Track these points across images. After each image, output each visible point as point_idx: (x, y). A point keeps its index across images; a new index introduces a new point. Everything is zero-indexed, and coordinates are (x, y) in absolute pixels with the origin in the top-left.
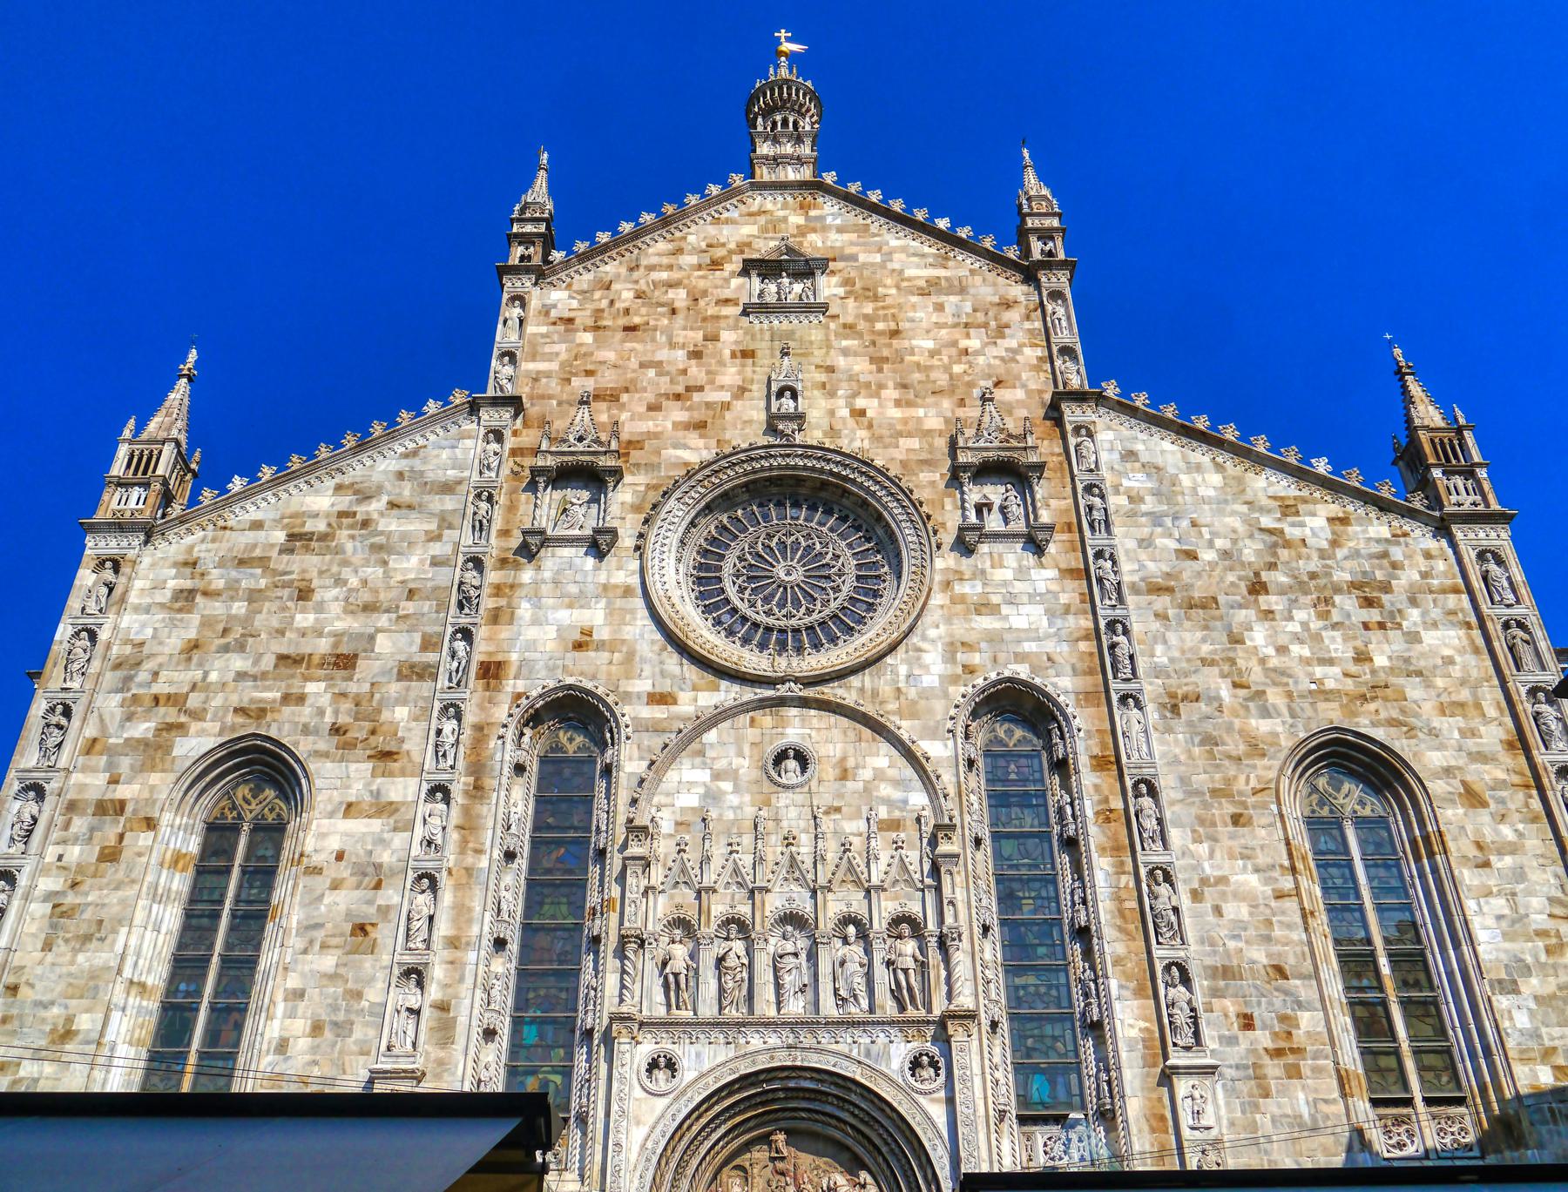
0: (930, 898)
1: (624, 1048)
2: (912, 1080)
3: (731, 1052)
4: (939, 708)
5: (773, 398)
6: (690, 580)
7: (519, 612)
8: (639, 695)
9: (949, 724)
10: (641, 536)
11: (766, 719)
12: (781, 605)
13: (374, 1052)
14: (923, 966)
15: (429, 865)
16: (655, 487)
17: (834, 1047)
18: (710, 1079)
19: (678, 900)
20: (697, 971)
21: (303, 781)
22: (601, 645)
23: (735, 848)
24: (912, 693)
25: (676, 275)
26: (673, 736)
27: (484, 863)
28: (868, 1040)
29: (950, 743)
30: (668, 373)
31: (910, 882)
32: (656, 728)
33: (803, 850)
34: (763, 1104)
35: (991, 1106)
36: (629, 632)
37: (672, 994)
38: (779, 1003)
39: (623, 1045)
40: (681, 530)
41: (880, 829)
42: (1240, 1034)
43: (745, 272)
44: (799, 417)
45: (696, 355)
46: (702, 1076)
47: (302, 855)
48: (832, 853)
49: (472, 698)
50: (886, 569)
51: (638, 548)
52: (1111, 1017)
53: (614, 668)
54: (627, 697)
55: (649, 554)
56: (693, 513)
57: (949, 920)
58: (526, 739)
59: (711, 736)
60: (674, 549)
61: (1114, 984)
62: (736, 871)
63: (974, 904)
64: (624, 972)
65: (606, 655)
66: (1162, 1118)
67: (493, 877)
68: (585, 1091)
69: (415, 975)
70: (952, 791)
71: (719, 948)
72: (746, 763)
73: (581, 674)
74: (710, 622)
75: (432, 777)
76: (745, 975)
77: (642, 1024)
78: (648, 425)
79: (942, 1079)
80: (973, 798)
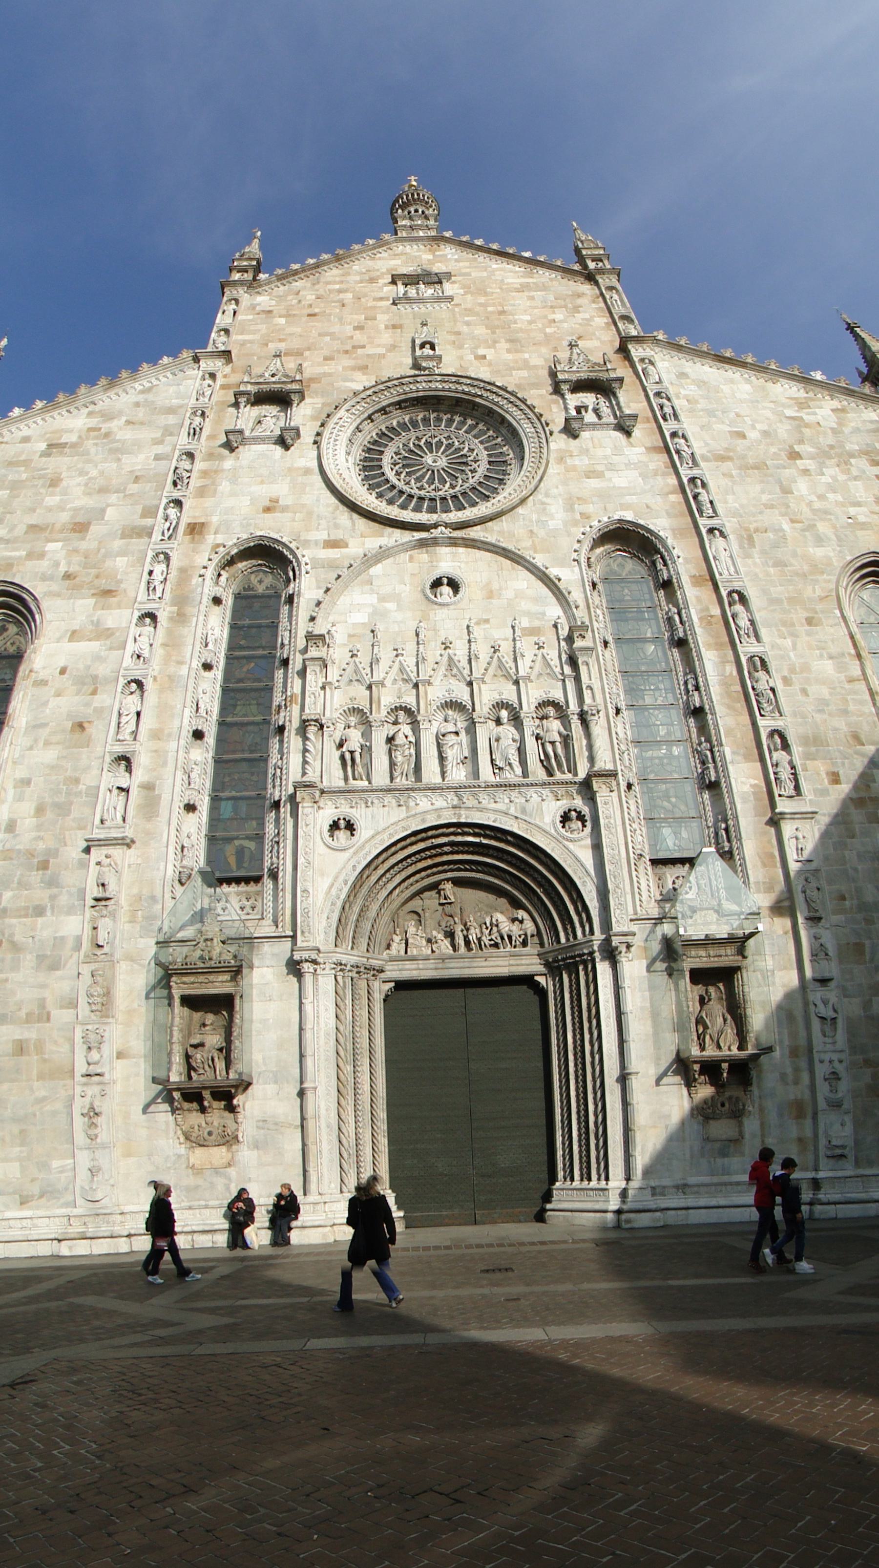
0: (570, 685)
1: (306, 811)
2: (563, 831)
3: (402, 813)
4: (567, 544)
5: (417, 348)
6: (358, 468)
7: (220, 488)
8: (316, 543)
9: (575, 555)
10: (318, 434)
11: (423, 556)
12: (431, 482)
13: (89, 827)
14: (566, 740)
15: (137, 674)
16: (329, 405)
17: (493, 806)
18: (385, 836)
19: (352, 694)
20: (370, 748)
21: (37, 617)
22: (285, 509)
23: (400, 651)
24: (542, 533)
25: (343, 286)
26: (345, 570)
27: (184, 671)
28: (523, 800)
29: (577, 569)
30: (339, 339)
31: (552, 675)
32: (331, 565)
33: (457, 652)
34: (430, 857)
35: (631, 850)
36: (308, 499)
37: (349, 769)
38: (443, 774)
39: (306, 809)
40: (350, 432)
41: (523, 635)
42: (830, 787)
43: (394, 282)
44: (439, 358)
45: (359, 328)
46: (378, 833)
47: (31, 671)
48: (483, 651)
49: (178, 549)
50: (511, 456)
51: (315, 442)
52: (727, 776)
53: (296, 523)
54: (306, 543)
55: (324, 445)
56: (358, 421)
57: (588, 700)
58: (223, 579)
59: (377, 570)
60: (344, 445)
61: (727, 750)
62: (402, 670)
63: (607, 690)
64: (305, 750)
65: (290, 515)
66: (772, 856)
67: (191, 681)
68: (275, 850)
69: (125, 761)
70: (582, 603)
71: (390, 730)
72: (408, 588)
73: (269, 529)
74: (374, 494)
75: (142, 606)
76: (413, 751)
77: (322, 792)
78: (326, 369)
79: (588, 829)
80: (599, 612)
